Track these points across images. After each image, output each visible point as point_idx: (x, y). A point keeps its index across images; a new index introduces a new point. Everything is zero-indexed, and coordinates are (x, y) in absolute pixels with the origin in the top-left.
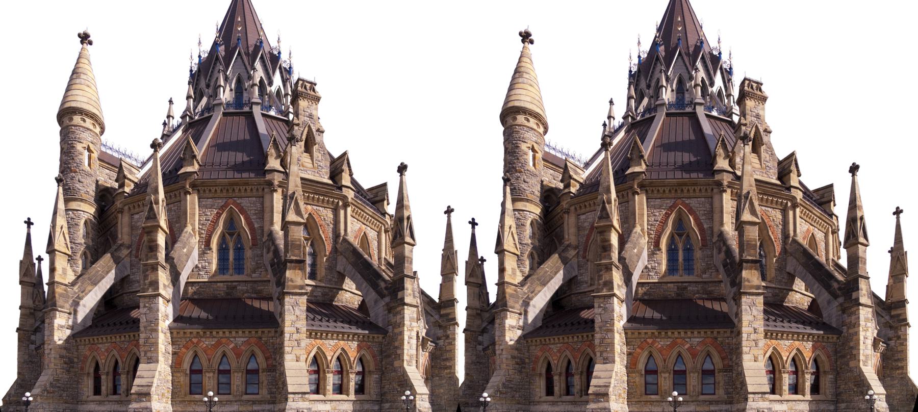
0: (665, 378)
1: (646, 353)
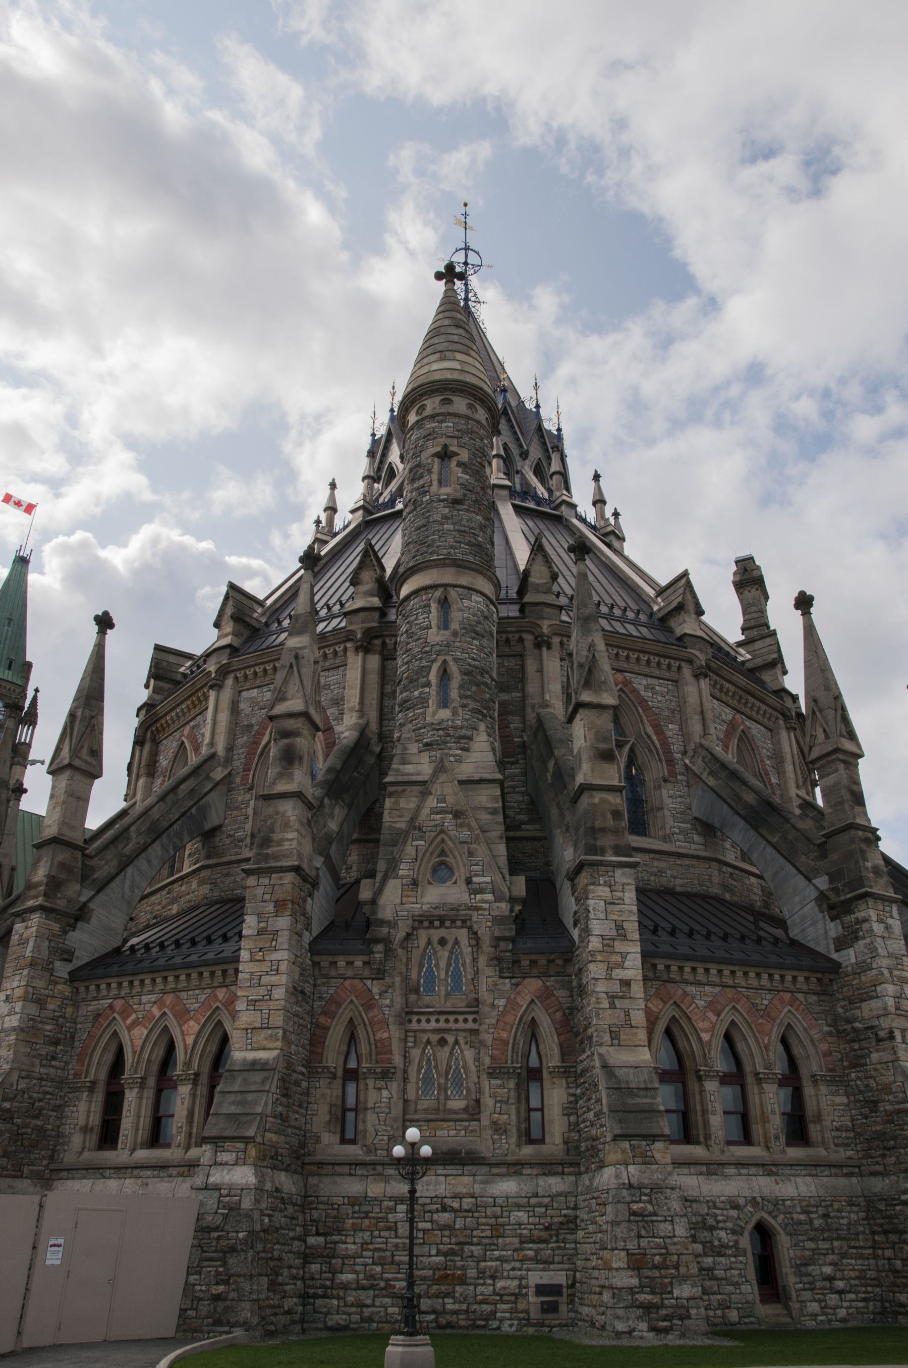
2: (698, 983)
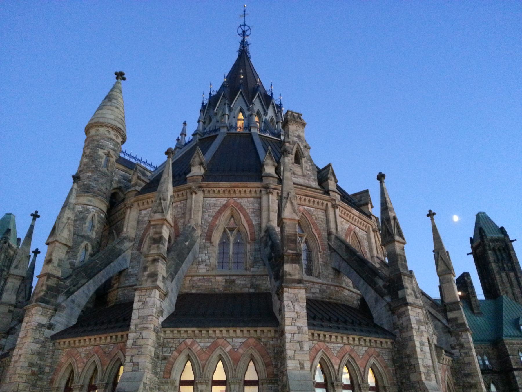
2: (83, 346)
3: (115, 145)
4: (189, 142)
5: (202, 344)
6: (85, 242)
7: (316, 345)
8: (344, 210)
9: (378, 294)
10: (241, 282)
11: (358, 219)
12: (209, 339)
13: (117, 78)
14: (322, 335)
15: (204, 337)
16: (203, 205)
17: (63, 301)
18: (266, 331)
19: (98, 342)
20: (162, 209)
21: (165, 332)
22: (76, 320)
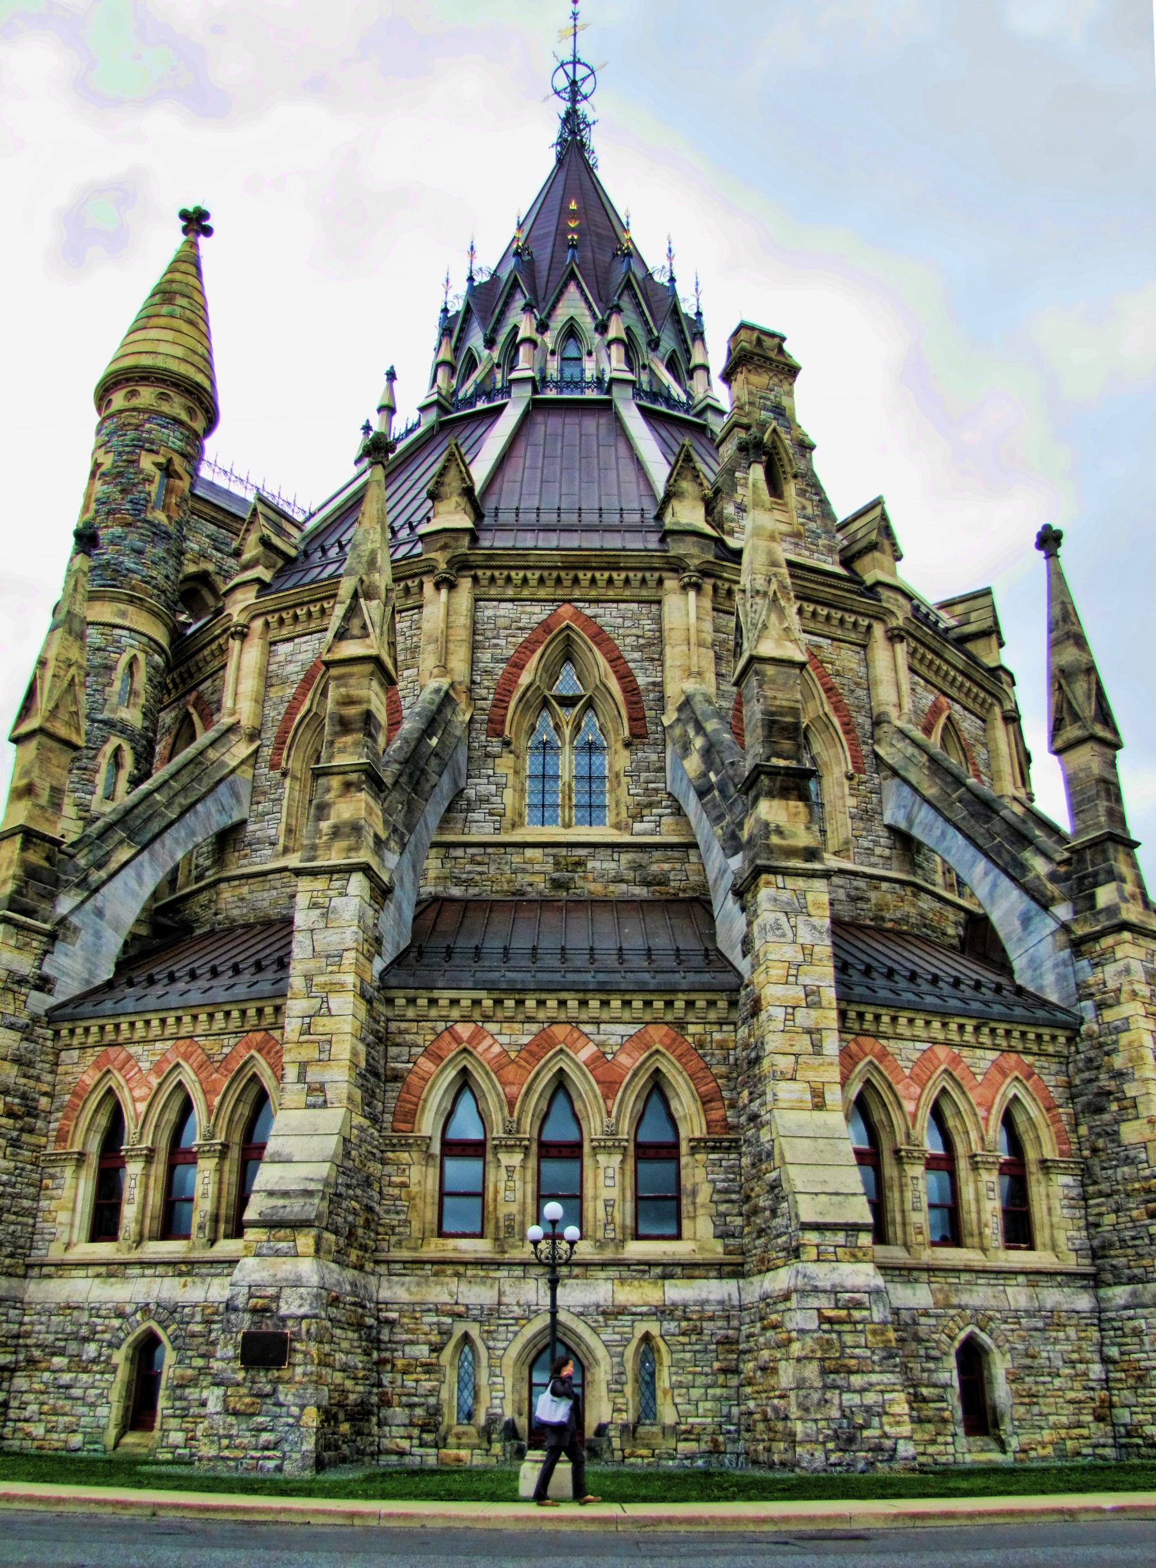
0: (510, 1170)
1: (451, 1073)
2: (144, 1041)
3: (187, 440)
4: (409, 432)
5: (504, 1039)
6: (115, 741)
7: (853, 1046)
8: (921, 650)
9: (1033, 898)
10: (605, 865)
11: (960, 678)
12: (527, 1026)
13: (185, 231)
14: (869, 1017)
15: (510, 1020)
16: (475, 623)
17: (72, 912)
18: (701, 1004)
19: (186, 1028)
20: (364, 627)
21: (390, 1002)
22: (112, 968)
